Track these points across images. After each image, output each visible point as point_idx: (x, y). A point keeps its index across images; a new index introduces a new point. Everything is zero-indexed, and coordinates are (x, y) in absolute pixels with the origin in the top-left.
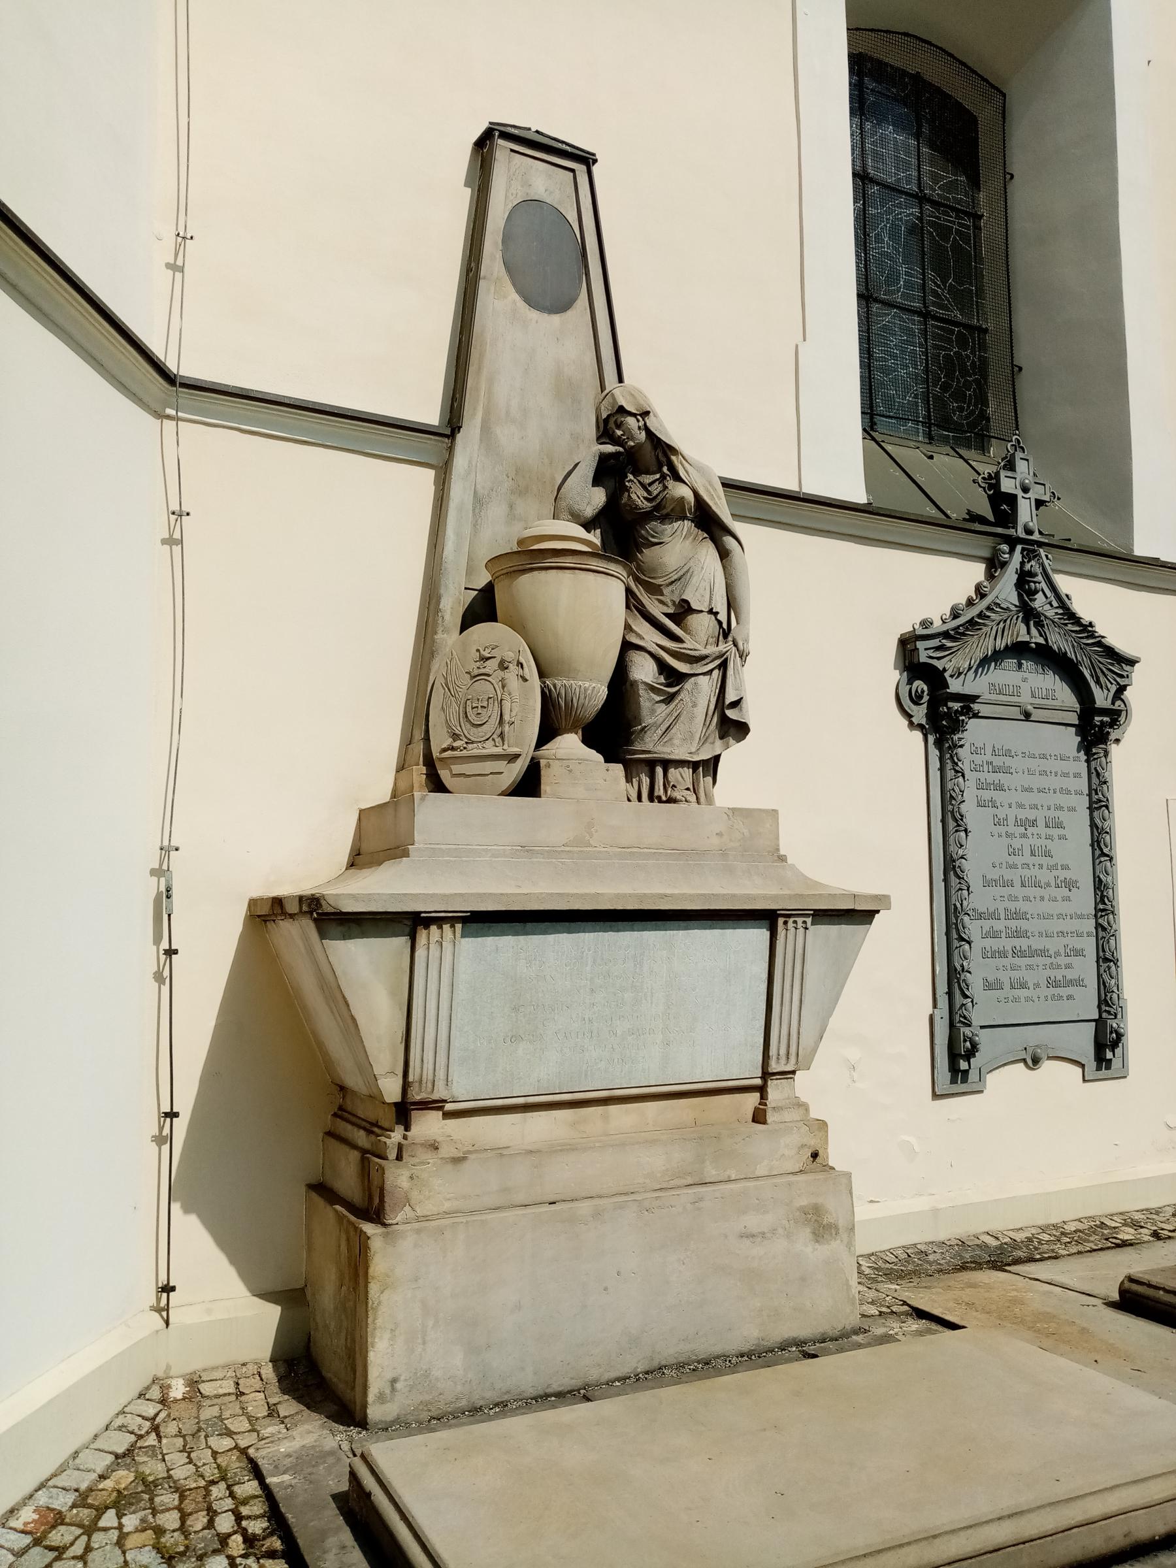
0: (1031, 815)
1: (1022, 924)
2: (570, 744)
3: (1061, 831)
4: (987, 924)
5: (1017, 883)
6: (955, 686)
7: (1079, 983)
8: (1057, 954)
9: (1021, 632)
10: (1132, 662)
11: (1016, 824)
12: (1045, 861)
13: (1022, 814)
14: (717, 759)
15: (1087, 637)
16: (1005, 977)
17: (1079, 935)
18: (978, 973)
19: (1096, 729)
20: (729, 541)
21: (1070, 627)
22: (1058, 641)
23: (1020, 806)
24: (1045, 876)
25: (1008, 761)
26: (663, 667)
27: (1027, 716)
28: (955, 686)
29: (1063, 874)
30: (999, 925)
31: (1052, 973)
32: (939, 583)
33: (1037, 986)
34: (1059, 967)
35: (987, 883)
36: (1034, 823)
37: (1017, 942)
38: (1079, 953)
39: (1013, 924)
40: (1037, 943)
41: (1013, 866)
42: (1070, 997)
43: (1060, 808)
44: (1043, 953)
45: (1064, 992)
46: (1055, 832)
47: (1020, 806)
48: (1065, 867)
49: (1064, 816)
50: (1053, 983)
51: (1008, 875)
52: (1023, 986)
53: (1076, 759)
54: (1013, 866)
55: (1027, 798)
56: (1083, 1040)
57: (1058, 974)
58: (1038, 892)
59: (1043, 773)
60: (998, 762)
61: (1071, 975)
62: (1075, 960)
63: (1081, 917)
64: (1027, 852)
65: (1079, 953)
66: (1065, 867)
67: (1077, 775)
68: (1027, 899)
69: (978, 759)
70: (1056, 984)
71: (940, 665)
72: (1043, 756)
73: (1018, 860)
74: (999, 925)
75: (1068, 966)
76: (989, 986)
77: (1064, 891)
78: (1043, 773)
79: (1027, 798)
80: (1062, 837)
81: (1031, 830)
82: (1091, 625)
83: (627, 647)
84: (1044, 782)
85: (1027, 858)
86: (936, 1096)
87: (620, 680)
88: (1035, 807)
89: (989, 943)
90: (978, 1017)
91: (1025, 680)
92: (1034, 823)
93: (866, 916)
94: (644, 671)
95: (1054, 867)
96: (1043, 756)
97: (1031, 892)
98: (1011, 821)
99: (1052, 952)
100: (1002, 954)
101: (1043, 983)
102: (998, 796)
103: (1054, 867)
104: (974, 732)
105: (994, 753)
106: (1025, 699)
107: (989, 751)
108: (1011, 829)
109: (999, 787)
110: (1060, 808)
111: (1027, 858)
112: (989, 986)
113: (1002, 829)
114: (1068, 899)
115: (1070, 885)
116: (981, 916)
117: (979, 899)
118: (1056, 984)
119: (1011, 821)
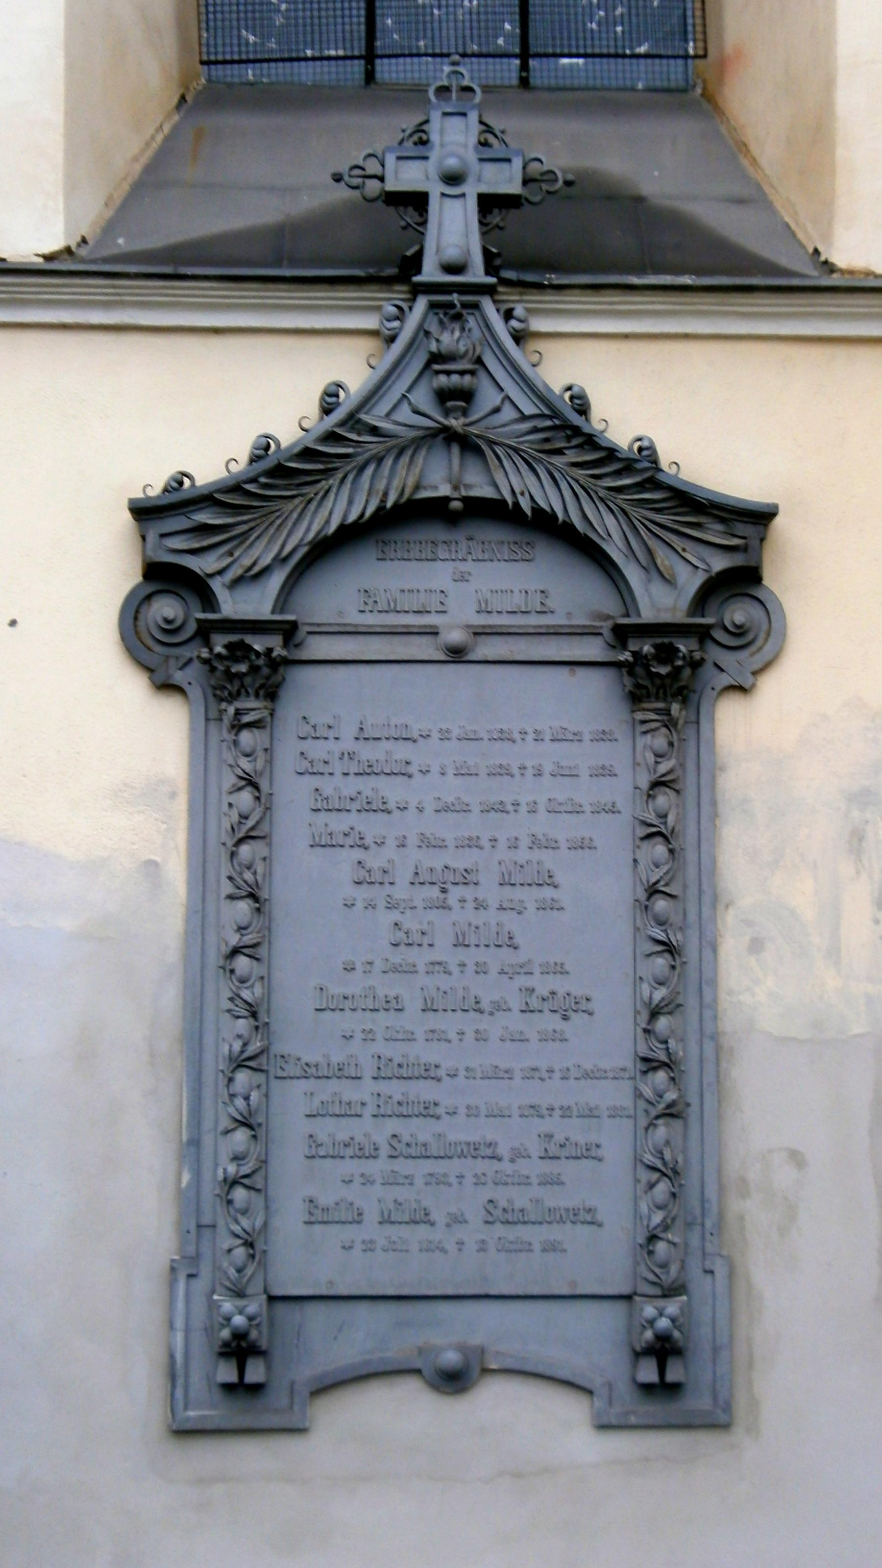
1: (425, 1091)
3: (547, 893)
4: (327, 1090)
5: (413, 1005)
8: (518, 1155)
9: (438, 476)
10: (761, 517)
12: (495, 959)
13: (436, 860)
15: (618, 473)
16: (371, 1201)
21: (572, 456)
23: (428, 843)
25: (402, 751)
27: (457, 655)
28: (233, 605)
29: (543, 985)
30: (349, 1092)
31: (502, 1195)
32: (243, 392)
33: (457, 1220)
34: (525, 1182)
37: (407, 1129)
38: (589, 1153)
39: (395, 1089)
40: (460, 1131)
42: (551, 1247)
43: (552, 845)
44: (472, 1151)
45: (535, 1235)
46: (530, 896)
47: (428, 843)
48: (560, 970)
50: (497, 1215)
52: (423, 1218)
53: (603, 737)
55: (449, 829)
56: (595, 1340)
57: (520, 1198)
58: (470, 1022)
59: (502, 772)
60: (368, 753)
62: (568, 1169)
64: (444, 940)
65: (589, 1153)
66: (560, 970)
67: (604, 772)
68: (435, 1036)
69: (318, 750)
70: (514, 1218)
72: (504, 737)
73: (421, 958)
77: (551, 1022)
78: (502, 772)
79: (449, 829)
80: (554, 906)
81: (456, 893)
85: (443, 951)
86: (184, 1432)
88: (472, 843)
89: (325, 1129)
91: (462, 578)
92: (467, 878)
95: (525, 969)
96: (504, 737)
97: (450, 1023)
98: (404, 875)
99: (503, 1150)
101: (475, 1215)
102: (371, 827)
103: (525, 969)
105: (362, 736)
107: (348, 732)
108: (400, 892)
110: (552, 845)
112: (317, 1215)
113: (378, 894)
114: (560, 1038)
115: (572, 1007)
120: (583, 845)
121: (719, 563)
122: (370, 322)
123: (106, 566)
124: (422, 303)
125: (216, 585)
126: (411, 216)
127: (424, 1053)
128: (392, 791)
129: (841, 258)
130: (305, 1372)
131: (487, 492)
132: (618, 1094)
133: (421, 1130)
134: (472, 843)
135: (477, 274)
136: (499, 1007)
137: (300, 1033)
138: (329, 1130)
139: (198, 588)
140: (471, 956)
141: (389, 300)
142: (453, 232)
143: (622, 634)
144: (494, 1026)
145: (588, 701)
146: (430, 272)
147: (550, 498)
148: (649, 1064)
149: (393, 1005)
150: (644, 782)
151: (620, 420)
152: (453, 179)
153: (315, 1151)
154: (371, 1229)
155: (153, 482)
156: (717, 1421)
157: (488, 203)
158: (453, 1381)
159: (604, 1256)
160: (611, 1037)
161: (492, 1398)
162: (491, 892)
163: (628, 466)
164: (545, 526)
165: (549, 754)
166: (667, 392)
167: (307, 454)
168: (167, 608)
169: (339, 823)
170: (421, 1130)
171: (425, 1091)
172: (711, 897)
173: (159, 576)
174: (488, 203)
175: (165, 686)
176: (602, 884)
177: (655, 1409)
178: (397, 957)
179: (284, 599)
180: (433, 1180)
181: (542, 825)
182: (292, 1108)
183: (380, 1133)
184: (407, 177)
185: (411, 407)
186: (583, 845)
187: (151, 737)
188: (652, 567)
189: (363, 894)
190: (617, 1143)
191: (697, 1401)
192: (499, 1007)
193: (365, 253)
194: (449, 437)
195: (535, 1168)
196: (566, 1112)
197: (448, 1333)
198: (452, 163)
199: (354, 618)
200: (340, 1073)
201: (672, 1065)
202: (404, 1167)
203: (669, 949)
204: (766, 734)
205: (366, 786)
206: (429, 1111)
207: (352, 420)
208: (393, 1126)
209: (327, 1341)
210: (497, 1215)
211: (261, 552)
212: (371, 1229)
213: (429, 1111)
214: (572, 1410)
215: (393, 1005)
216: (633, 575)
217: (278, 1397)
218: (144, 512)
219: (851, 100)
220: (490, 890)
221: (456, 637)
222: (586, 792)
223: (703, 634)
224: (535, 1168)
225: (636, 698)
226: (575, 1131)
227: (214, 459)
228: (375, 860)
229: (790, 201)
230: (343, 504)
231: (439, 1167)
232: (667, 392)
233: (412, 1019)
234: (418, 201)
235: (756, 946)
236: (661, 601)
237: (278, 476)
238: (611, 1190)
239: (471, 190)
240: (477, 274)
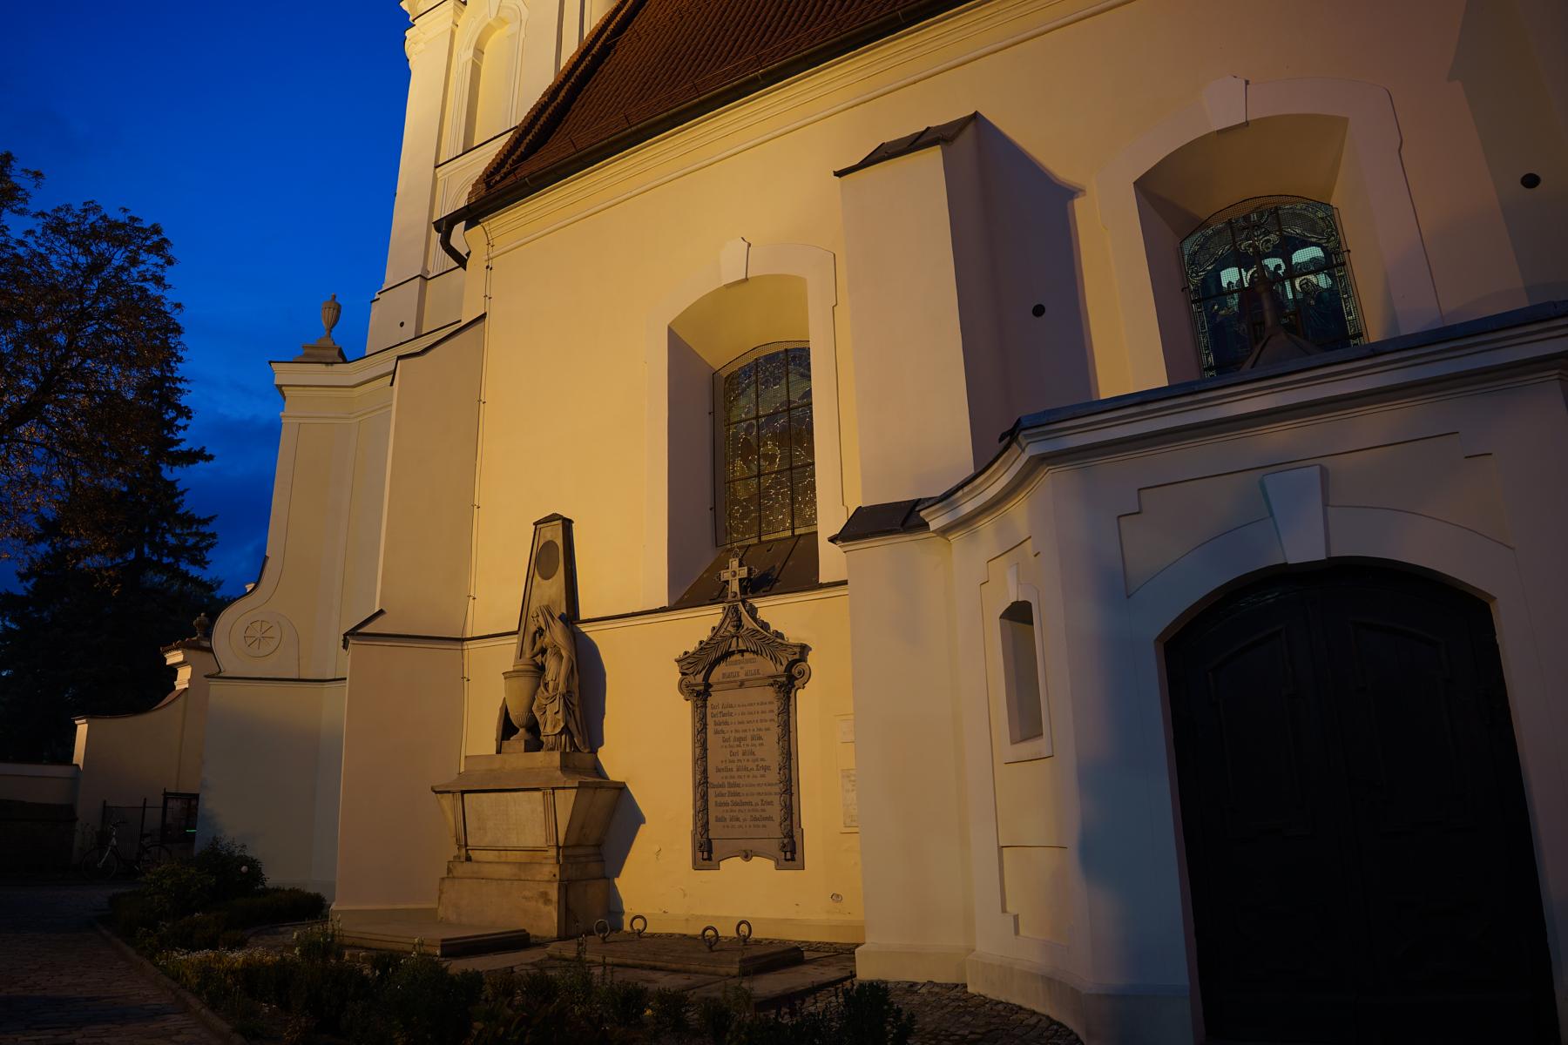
0: (742, 735)
4: (719, 790)
16: (727, 816)
18: (713, 812)
24: (751, 765)
27: (742, 685)
30: (725, 791)
35: (719, 770)
36: (744, 739)
38: (770, 803)
40: (745, 799)
44: (749, 803)
51: (730, 766)
55: (740, 727)
56: (775, 846)
61: (764, 815)
62: (768, 808)
65: (770, 803)
70: (756, 819)
74: (725, 791)
76: (718, 820)
79: (740, 727)
84: (749, 718)
85: (740, 756)
89: (719, 799)
92: (744, 739)
100: (726, 804)
104: (715, 699)
106: (742, 677)
109: (726, 723)
111: (740, 756)
112: (718, 820)
115: (766, 768)
117: (713, 778)
118: (756, 819)
127: (738, 781)
138: (719, 799)
158: (747, 857)
160: (774, 776)
165: (760, 708)
179: (706, 678)
181: (760, 725)
183: (728, 799)
200: (722, 786)
206: (738, 794)
213: (738, 794)
220: (749, 741)
222: (768, 716)
226: (769, 798)
238: (776, 811)
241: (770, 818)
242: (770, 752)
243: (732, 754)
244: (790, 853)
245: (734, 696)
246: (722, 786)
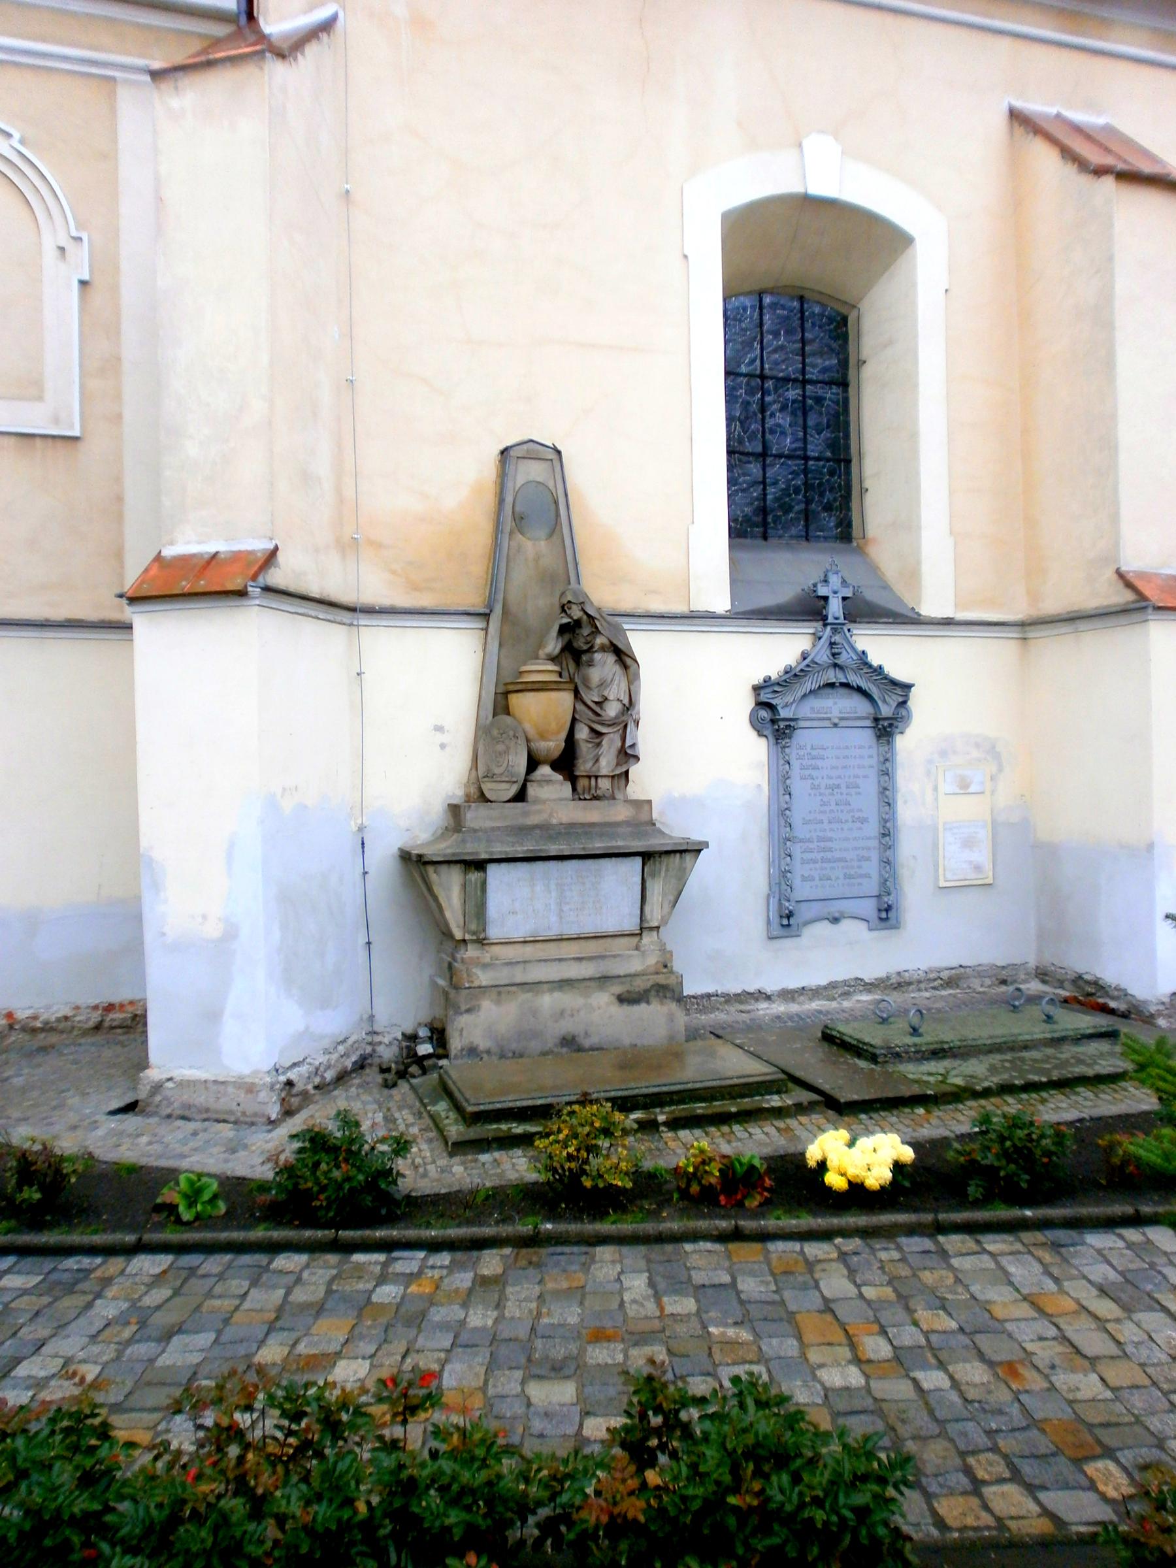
0: (836, 782)
1: (829, 844)
2: (545, 770)
4: (804, 845)
5: (826, 822)
6: (783, 713)
7: (868, 876)
9: (832, 676)
10: (908, 687)
11: (826, 787)
13: (831, 782)
14: (627, 773)
17: (869, 849)
19: (886, 729)
20: (629, 661)
22: (854, 679)
25: (822, 752)
26: (592, 730)
27: (835, 725)
28: (783, 713)
29: (857, 815)
30: (811, 846)
33: (838, 878)
34: (853, 867)
39: (822, 844)
40: (837, 855)
41: (825, 812)
42: (860, 884)
46: (853, 791)
48: (860, 810)
49: (859, 781)
50: (846, 876)
51: (820, 817)
53: (870, 747)
54: (825, 812)
56: (869, 908)
59: (846, 757)
60: (814, 753)
62: (865, 864)
63: (869, 838)
64: (833, 803)
65: (868, 859)
66: (860, 810)
67: (870, 757)
68: (832, 830)
69: (802, 752)
70: (851, 877)
71: (774, 702)
72: (847, 747)
73: (827, 809)
75: (860, 867)
77: (858, 825)
78: (846, 757)
82: (880, 667)
83: (574, 720)
85: (833, 807)
86: (771, 938)
87: (570, 739)
88: (840, 777)
89: (807, 856)
90: (798, 895)
92: (838, 786)
93: (699, 851)
94: (582, 733)
95: (852, 811)
96: (847, 747)
97: (834, 826)
98: (823, 786)
100: (815, 861)
101: (841, 876)
102: (814, 773)
103: (852, 811)
104: (803, 738)
105: (812, 748)
107: (809, 747)
108: (822, 791)
109: (816, 768)
111: (833, 807)
112: (804, 879)
114: (861, 829)
115: (864, 821)
116: (801, 841)
119: (823, 786)
120: (865, 777)
121: (901, 699)
122: (812, 631)
123: (747, 703)
124: (829, 628)
125: (779, 708)
126: (822, 602)
127: (829, 834)
128: (819, 763)
129: (923, 612)
130: (801, 921)
131: (844, 681)
132: (874, 843)
133: (829, 855)
134: (840, 777)
135: (842, 620)
136: (847, 821)
137: (800, 831)
138: (807, 856)
139: (770, 707)
140: (839, 808)
141: (819, 625)
142: (835, 608)
143: (876, 720)
144: (845, 826)
145: (865, 737)
146: (830, 620)
147: (864, 685)
148: (884, 835)
149: (822, 822)
150: (882, 759)
151: (874, 659)
152: (835, 593)
153: (803, 862)
154: (817, 882)
155: (758, 679)
156: (896, 927)
157: (844, 599)
158: (835, 920)
159: (871, 886)
161: (846, 924)
162: (844, 790)
163: (875, 670)
164: (859, 690)
166: (883, 648)
167: (802, 670)
168: (764, 714)
169: (807, 772)
170: (829, 855)
171: (829, 844)
172: (894, 789)
173: (761, 704)
174: (844, 599)
175: (760, 734)
176: (870, 787)
177: (883, 925)
178: (822, 809)
180: (832, 868)
182: (797, 850)
184: (822, 591)
185: (824, 657)
186: (865, 777)
187: (758, 748)
188: (885, 701)
189: (813, 792)
190: (875, 856)
191: (892, 922)
192: (847, 821)
193: (810, 609)
194: (835, 665)
195: (855, 864)
196: (863, 849)
197: (835, 908)
198: (835, 588)
199: (809, 715)
200: (810, 841)
201: (887, 833)
202: (825, 865)
203: (889, 804)
204: (905, 743)
205: (813, 762)
206: (830, 850)
207: (813, 662)
208: (822, 854)
209: (805, 912)
210: (846, 876)
211: (789, 698)
212: (817, 882)
213: (830, 850)
214: (863, 926)
215: (822, 822)
216: (880, 703)
217: (794, 928)
218: (757, 689)
219: (925, 568)
220: (844, 790)
221: (836, 721)
222: (867, 762)
223: (895, 719)
224: (855, 864)
225: (879, 737)
226: (865, 853)
227: (774, 669)
228: (816, 782)
229: (900, 589)
230: (808, 685)
231: (835, 865)
232: (883, 648)
233: (826, 825)
234: (826, 599)
235: (905, 802)
236: (886, 711)
237: (791, 677)
238: (872, 868)
239: (840, 595)
240: (842, 620)
241: (868, 876)
242: (867, 801)
243: (824, 804)
244: (886, 914)
245: (829, 737)
246: (810, 841)
